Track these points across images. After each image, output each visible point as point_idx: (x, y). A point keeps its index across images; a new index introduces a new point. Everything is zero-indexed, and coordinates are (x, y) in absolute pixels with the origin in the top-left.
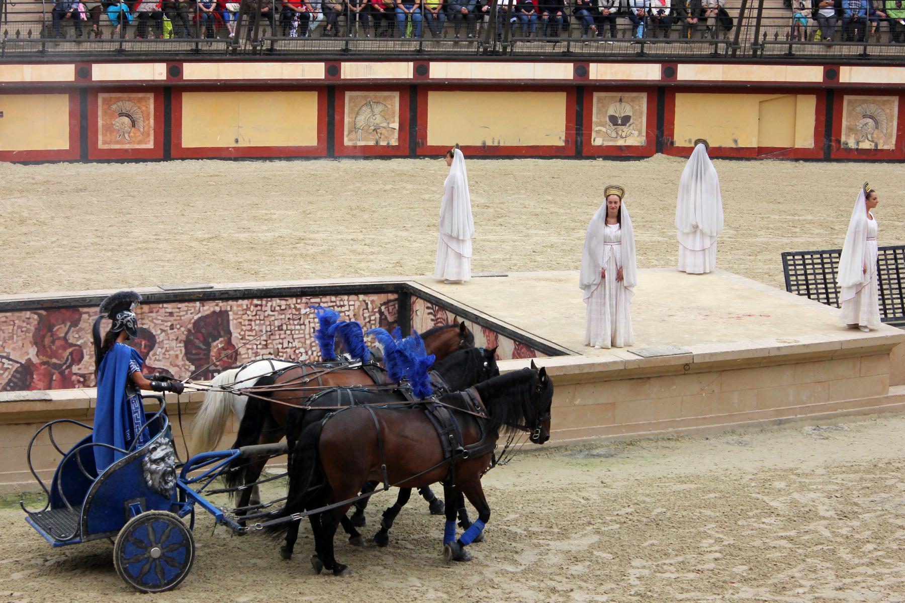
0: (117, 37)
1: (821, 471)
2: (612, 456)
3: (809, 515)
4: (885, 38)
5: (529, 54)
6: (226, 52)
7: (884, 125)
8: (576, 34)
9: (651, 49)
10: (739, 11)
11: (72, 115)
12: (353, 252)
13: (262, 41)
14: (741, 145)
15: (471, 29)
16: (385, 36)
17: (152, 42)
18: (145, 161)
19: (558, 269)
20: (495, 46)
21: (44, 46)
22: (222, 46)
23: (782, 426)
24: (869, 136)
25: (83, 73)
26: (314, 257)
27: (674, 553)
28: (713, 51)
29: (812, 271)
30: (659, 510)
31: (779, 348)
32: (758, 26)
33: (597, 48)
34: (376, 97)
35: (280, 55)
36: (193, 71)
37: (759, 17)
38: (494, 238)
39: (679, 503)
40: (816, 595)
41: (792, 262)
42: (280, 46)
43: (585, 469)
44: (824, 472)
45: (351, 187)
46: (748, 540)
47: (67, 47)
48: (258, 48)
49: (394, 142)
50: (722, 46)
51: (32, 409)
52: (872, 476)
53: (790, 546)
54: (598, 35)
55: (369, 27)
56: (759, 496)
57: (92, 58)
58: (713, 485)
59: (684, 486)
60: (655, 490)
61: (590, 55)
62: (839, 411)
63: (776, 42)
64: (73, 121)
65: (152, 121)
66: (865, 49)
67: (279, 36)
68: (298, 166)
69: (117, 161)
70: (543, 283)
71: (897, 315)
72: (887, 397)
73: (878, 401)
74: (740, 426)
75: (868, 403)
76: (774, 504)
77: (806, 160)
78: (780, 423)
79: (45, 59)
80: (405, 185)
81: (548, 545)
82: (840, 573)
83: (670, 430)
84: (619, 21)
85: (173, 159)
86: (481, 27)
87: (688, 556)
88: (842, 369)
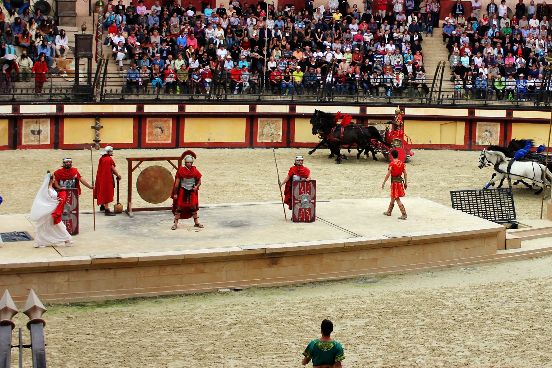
0: (156, 93)
1: (467, 288)
2: (376, 282)
3: (461, 308)
4: (494, 98)
5: (340, 102)
6: (205, 100)
7: (494, 135)
8: (361, 94)
9: (394, 101)
10: (431, 85)
11: (134, 128)
12: (261, 190)
13: (222, 95)
14: (433, 143)
15: (314, 91)
16: (276, 94)
17: (171, 95)
18: (167, 148)
19: (353, 198)
20: (325, 99)
21: (123, 97)
22: (203, 97)
23: (450, 268)
24: (488, 140)
25: (140, 108)
26: (242, 192)
27: (403, 326)
28: (420, 102)
29: (463, 199)
30: (396, 307)
31: (449, 234)
32: (440, 91)
33: (370, 100)
34: (272, 121)
35: (229, 101)
36: (190, 108)
37: (440, 88)
38: (324, 184)
39: (405, 303)
40: (465, 344)
41: (455, 195)
42: (229, 97)
43: (363, 288)
44: (469, 288)
45: (260, 161)
46: (435, 320)
47: (133, 97)
48: (220, 98)
49: (280, 141)
50: (424, 100)
51: (112, 262)
52: (489, 290)
53: (454, 322)
54: (370, 94)
55: (269, 90)
56: (440, 300)
57: (144, 102)
58: (420, 295)
59: (408, 296)
60: (395, 298)
61: (367, 103)
62: (475, 261)
63: (447, 99)
64: (135, 130)
65: (171, 130)
66: (486, 102)
67: (229, 93)
68: (237, 151)
69: (154, 148)
70: (346, 204)
71: (500, 219)
72: (496, 255)
73: (492, 257)
74: (433, 268)
75: (488, 258)
76: (447, 303)
77: (461, 150)
78: (450, 267)
79: (123, 103)
80: (284, 160)
81: (347, 323)
82: (476, 334)
83: (401, 270)
84: (380, 88)
85: (180, 148)
86: (319, 90)
87: (409, 328)
88: (477, 243)
